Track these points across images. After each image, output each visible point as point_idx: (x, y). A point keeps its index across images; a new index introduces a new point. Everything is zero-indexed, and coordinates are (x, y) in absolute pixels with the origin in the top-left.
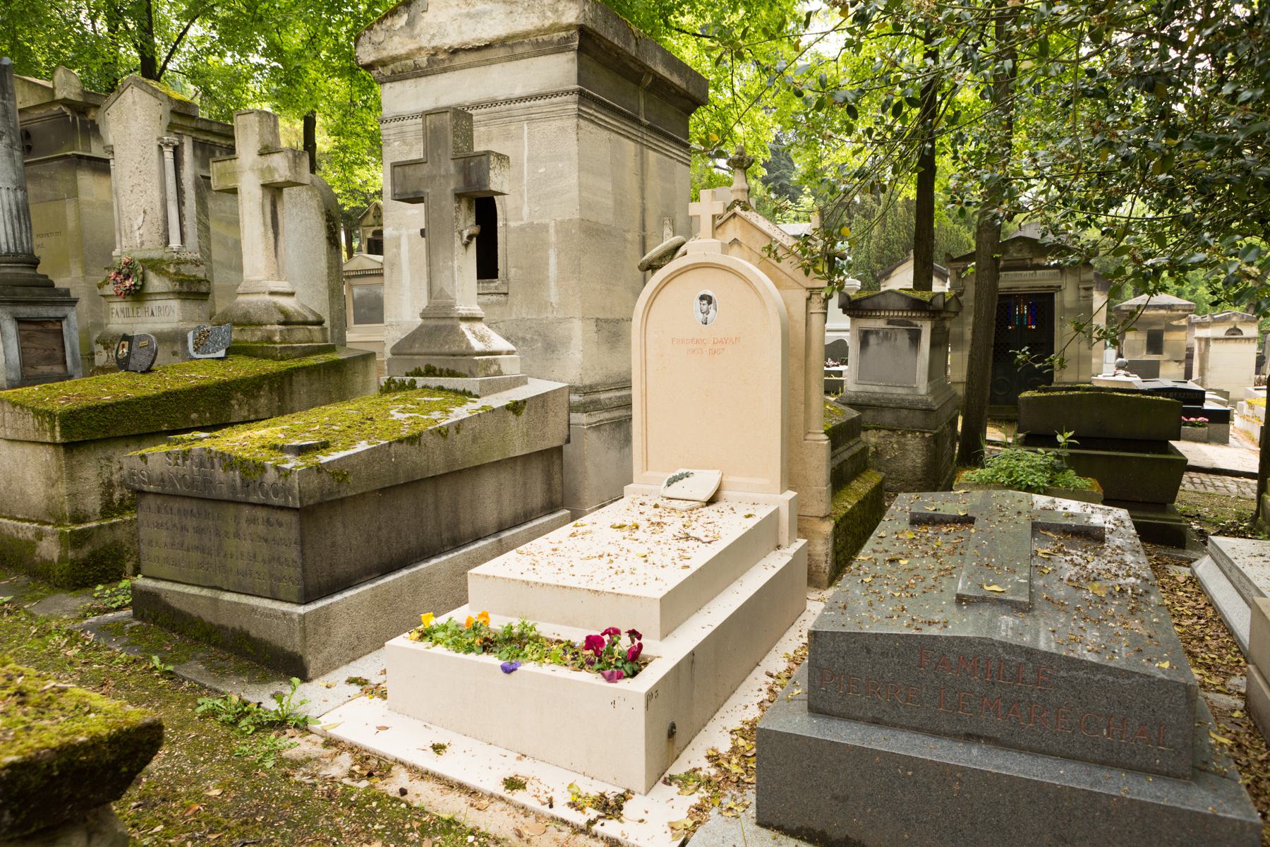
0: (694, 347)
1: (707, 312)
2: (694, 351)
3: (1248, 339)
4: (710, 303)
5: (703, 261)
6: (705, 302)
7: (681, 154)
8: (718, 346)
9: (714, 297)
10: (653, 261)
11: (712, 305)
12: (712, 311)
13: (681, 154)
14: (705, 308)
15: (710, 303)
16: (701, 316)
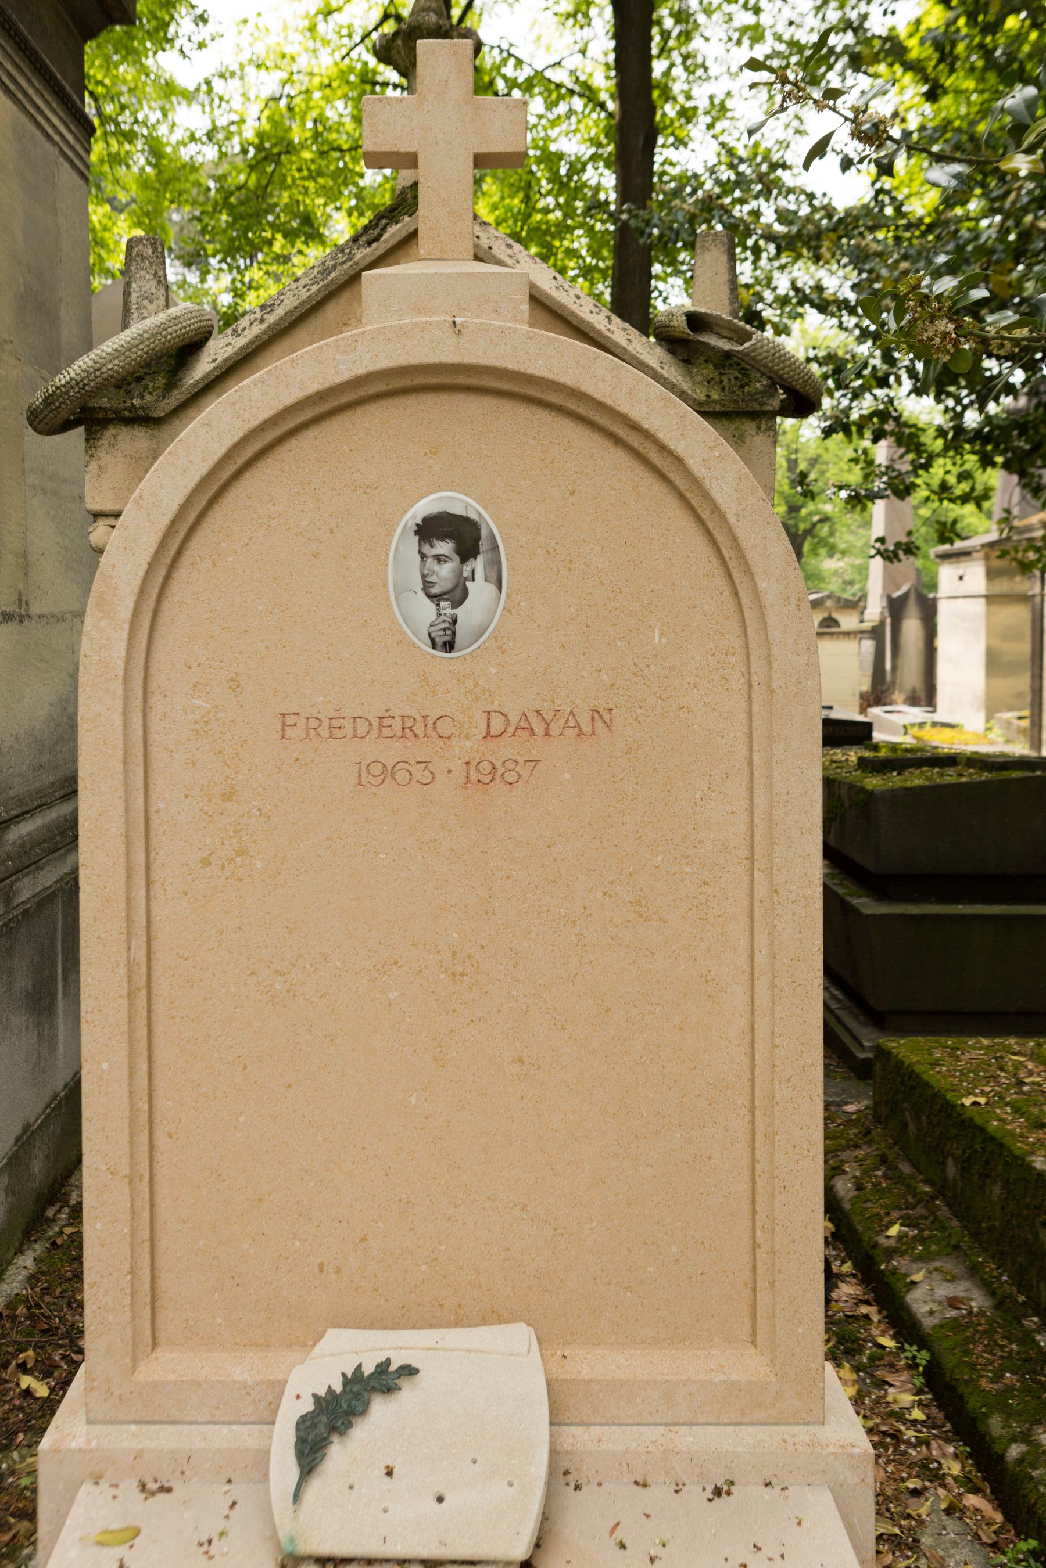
0: (394, 751)
1: (458, 595)
2: (389, 773)
3: (848, 634)
4: (467, 550)
5: (448, 355)
6: (444, 547)
7: (70, 138)
8: (507, 749)
9: (489, 522)
10: (100, 389)
11: (479, 564)
12: (480, 591)
13: (70, 138)
14: (444, 574)
15: (467, 550)
16: (425, 611)
